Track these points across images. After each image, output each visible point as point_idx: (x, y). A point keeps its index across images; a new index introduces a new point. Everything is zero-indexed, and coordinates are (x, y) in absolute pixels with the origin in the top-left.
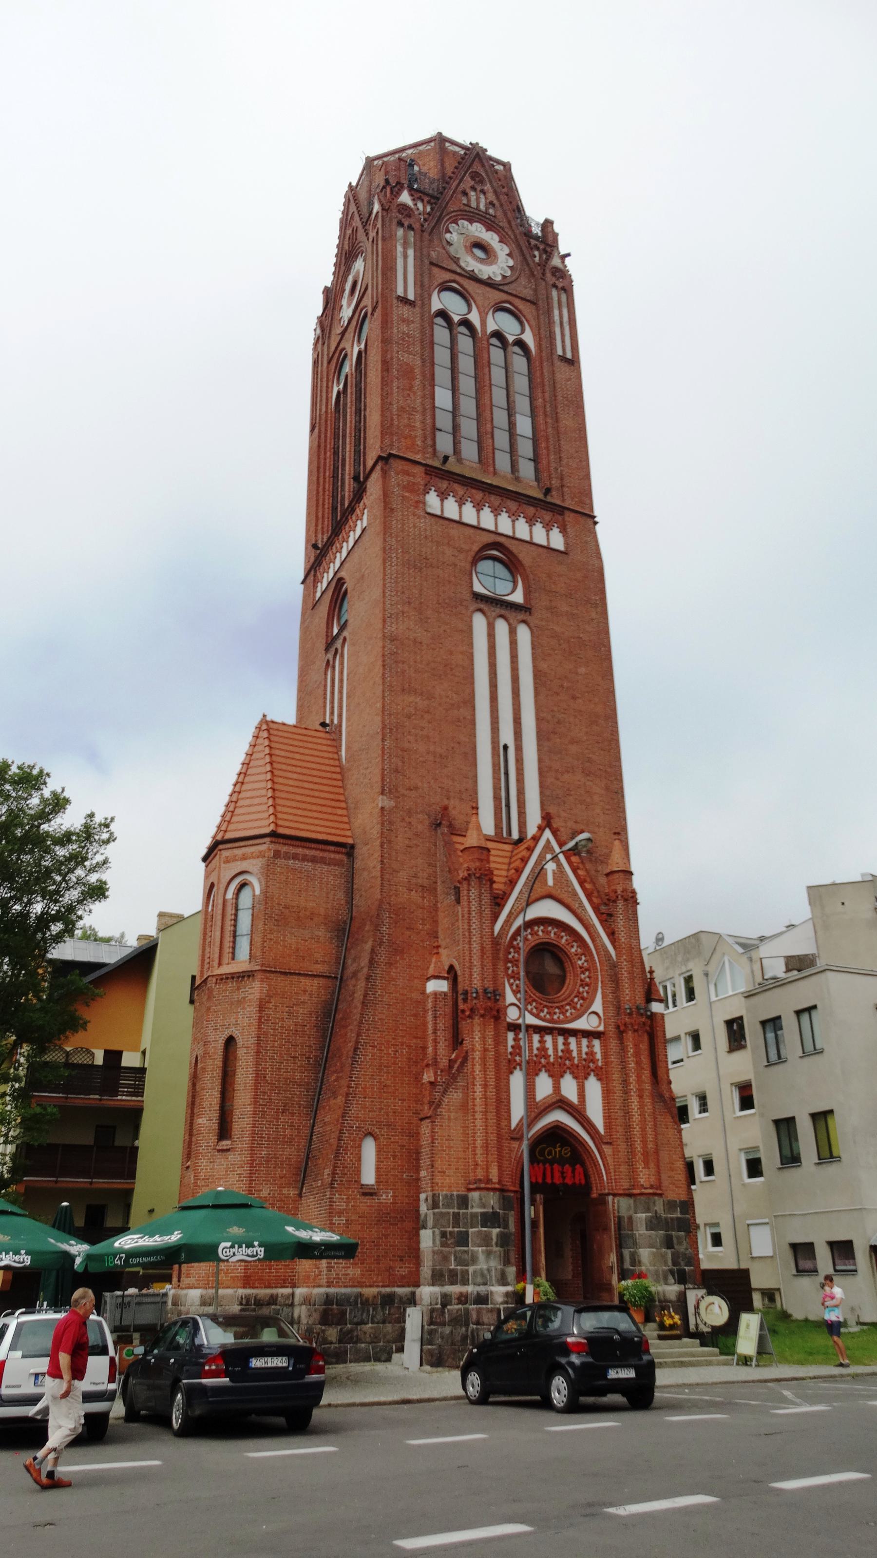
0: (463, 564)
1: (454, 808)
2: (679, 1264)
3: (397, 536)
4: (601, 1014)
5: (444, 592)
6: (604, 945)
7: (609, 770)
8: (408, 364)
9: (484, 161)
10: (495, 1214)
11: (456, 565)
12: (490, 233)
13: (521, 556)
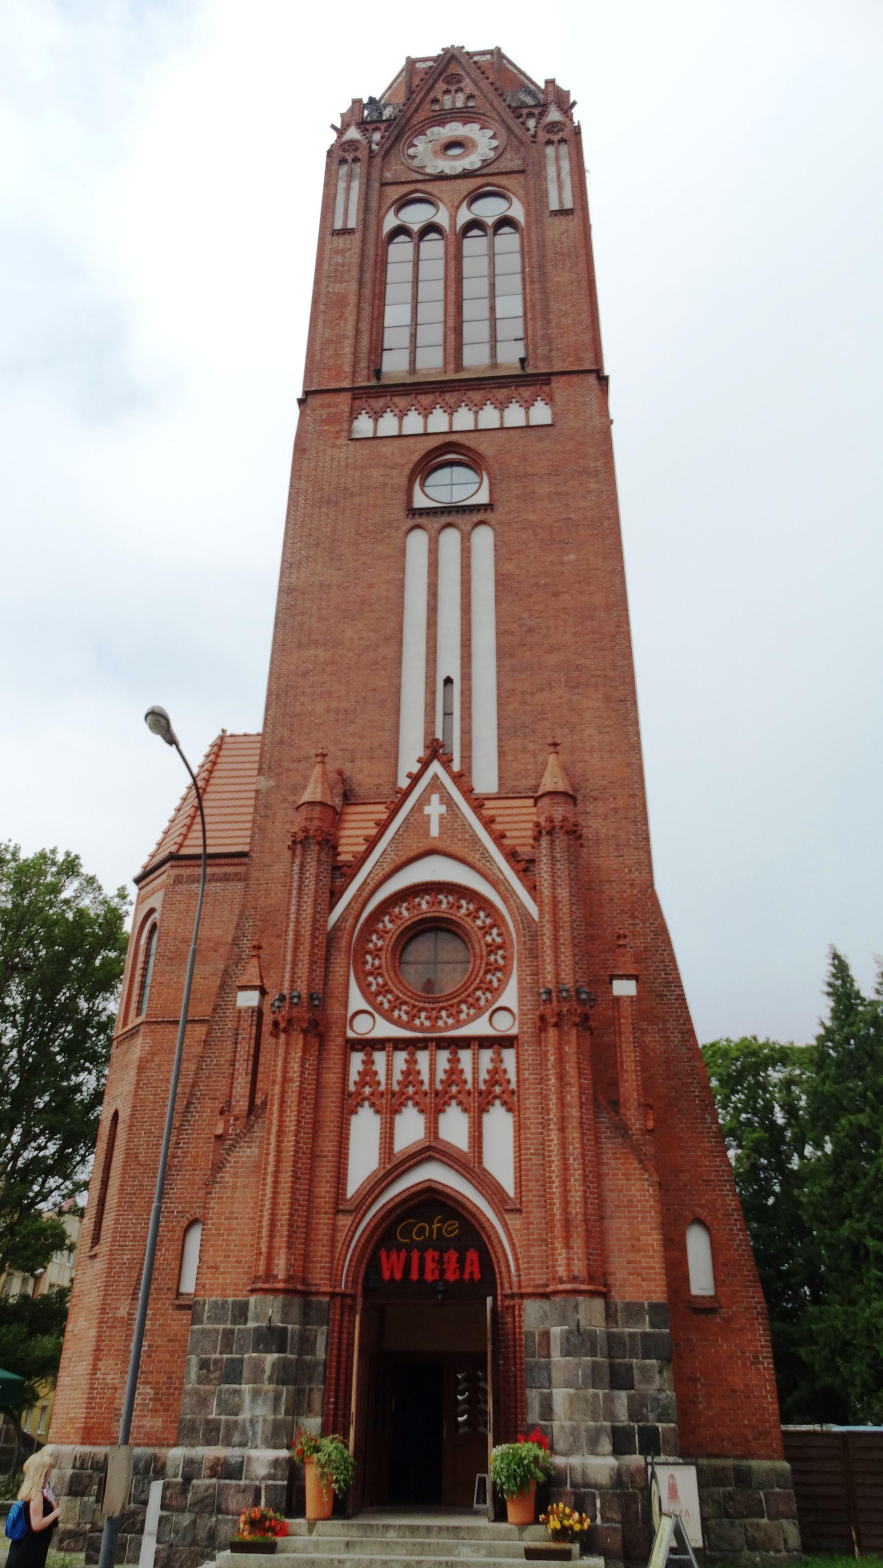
0: (396, 481)
1: (361, 771)
2: (647, 1420)
3: (307, 476)
4: (515, 1010)
5: (367, 520)
6: (521, 907)
7: (611, 673)
8: (337, 294)
9: (463, 61)
10: (270, 1329)
11: (385, 485)
12: (468, 126)
13: (481, 449)
